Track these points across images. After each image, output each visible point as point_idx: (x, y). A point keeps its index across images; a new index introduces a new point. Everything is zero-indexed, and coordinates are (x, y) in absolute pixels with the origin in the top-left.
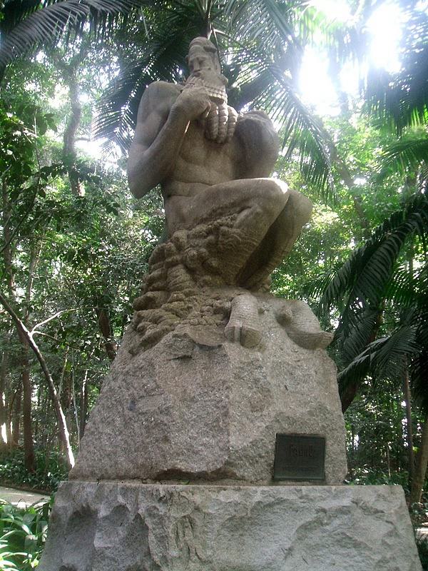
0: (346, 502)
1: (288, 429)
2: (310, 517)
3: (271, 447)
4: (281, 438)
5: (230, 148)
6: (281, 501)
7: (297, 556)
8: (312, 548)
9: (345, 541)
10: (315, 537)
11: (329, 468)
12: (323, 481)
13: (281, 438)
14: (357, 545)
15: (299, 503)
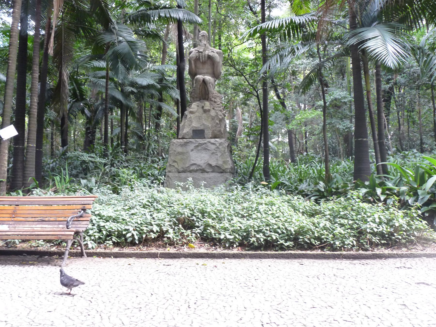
0: (205, 142)
1: (195, 129)
2: (197, 144)
3: (191, 132)
4: (194, 131)
5: (209, 62)
6: (191, 142)
7: (194, 151)
8: (198, 150)
9: (205, 149)
10: (199, 148)
11: (206, 136)
12: (204, 138)
13: (194, 131)
14: (208, 150)
15: (195, 142)
